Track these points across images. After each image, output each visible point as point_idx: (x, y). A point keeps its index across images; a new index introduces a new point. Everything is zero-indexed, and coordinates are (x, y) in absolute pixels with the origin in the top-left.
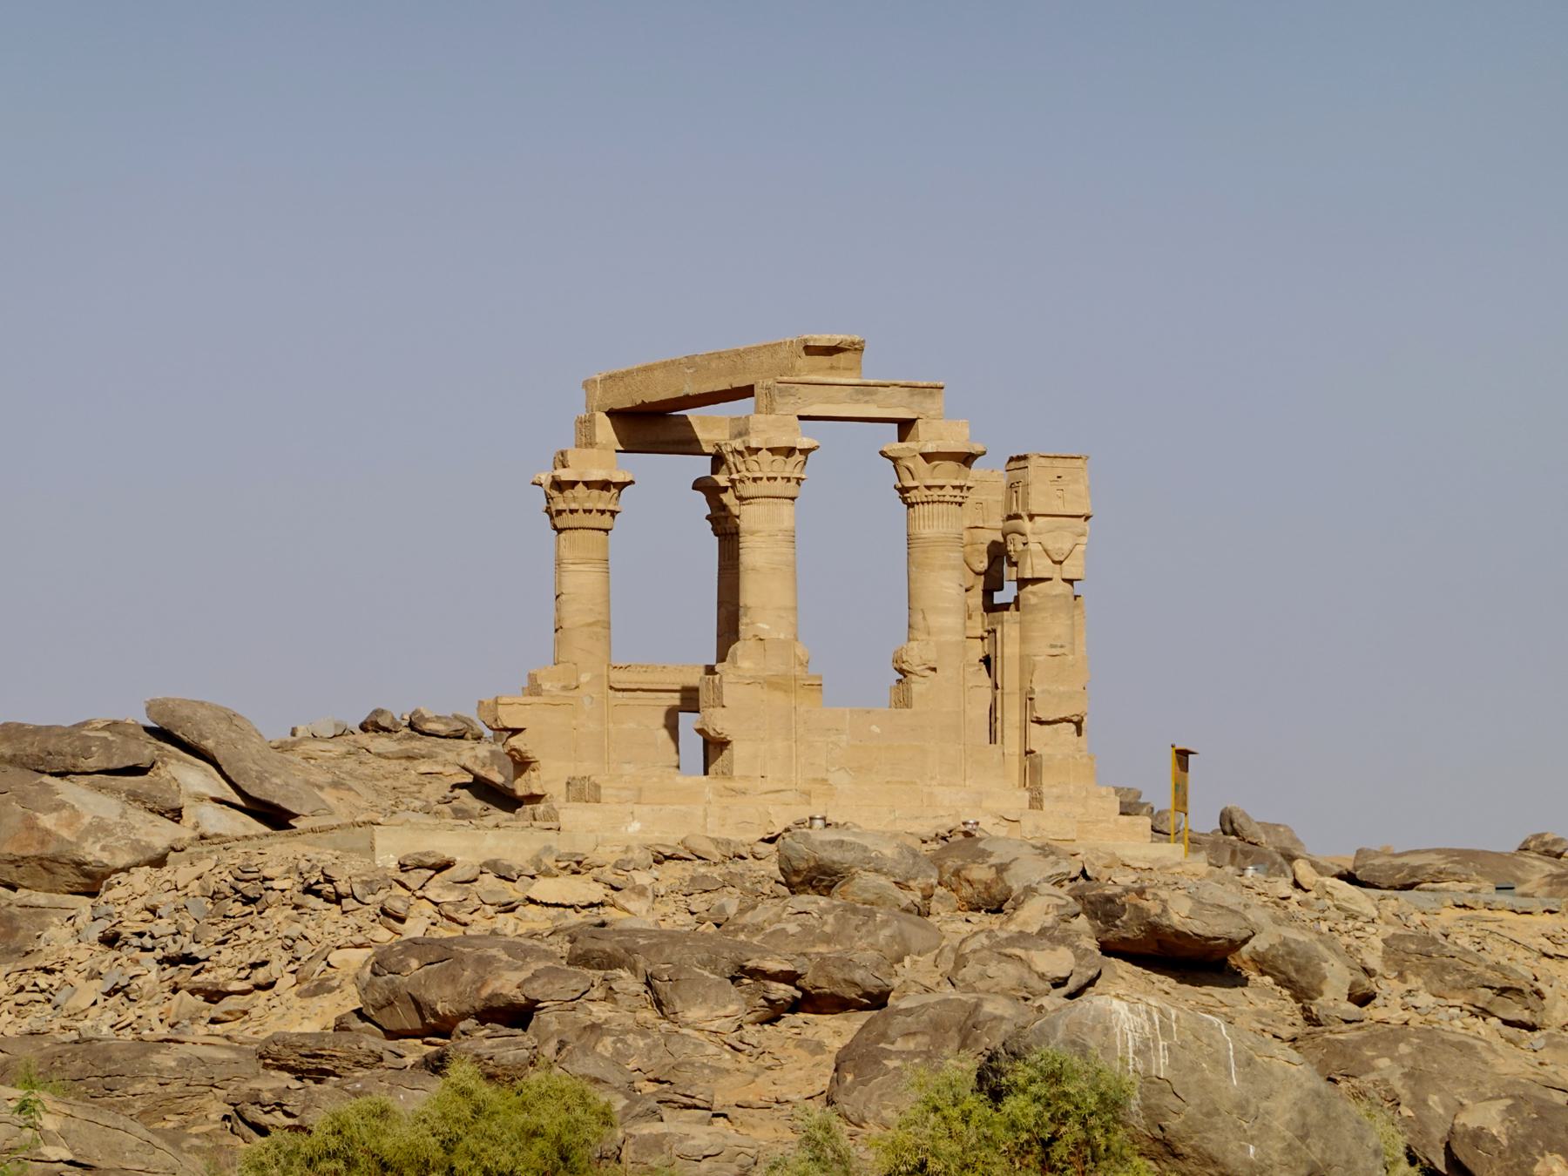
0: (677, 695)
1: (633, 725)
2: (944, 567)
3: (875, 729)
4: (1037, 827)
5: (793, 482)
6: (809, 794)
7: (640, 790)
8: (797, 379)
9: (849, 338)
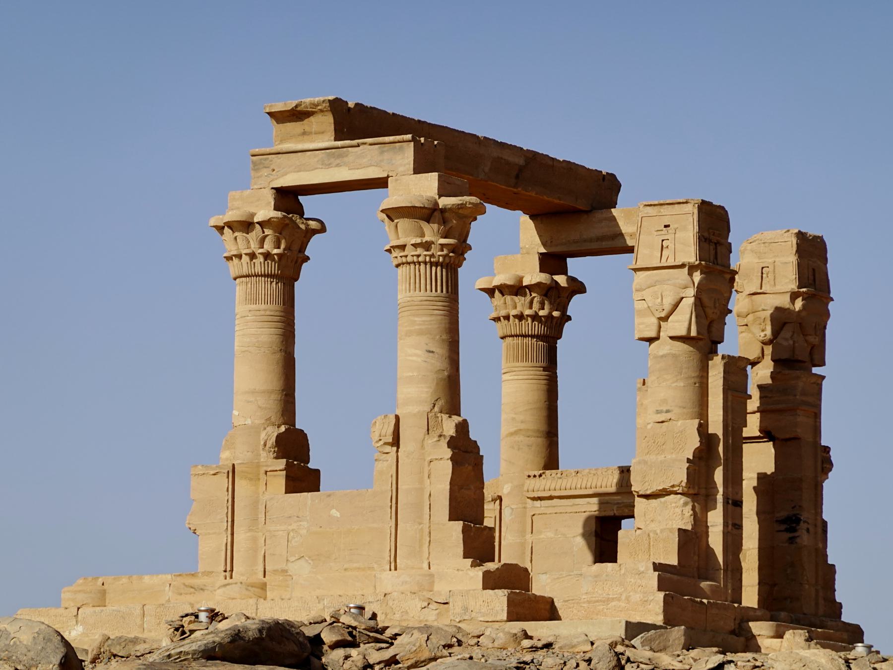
0: (595, 500)
1: (550, 534)
2: (409, 334)
3: (335, 513)
4: (466, 609)
5: (245, 259)
6: (263, 587)
7: (103, 593)
8: (268, 150)
9: (308, 100)
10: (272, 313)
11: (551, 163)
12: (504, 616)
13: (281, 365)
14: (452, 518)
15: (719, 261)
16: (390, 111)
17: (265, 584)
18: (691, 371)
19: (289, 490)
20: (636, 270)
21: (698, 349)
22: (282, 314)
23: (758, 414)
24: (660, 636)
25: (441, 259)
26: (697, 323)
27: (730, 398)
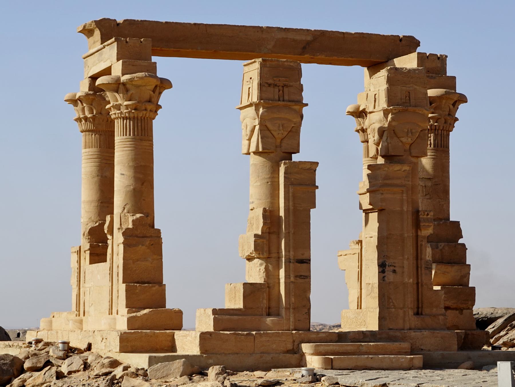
6: (81, 322)
10: (92, 154)
11: (342, 35)
12: (118, 350)
13: (97, 185)
14: (123, 283)
15: (286, 98)
16: (164, 21)
17: (82, 321)
18: (265, 174)
19: (91, 263)
20: (241, 109)
21: (269, 160)
22: (99, 153)
23: (368, 194)
24: (164, 367)
25: (127, 115)
26: (262, 142)
27: (291, 190)
